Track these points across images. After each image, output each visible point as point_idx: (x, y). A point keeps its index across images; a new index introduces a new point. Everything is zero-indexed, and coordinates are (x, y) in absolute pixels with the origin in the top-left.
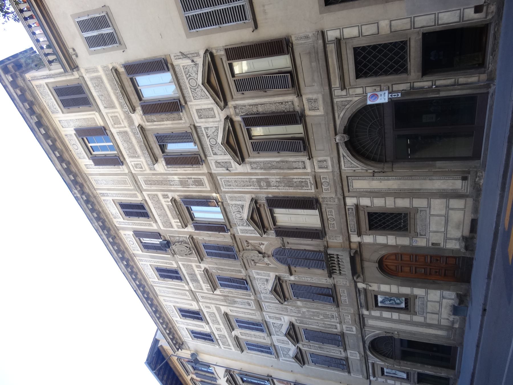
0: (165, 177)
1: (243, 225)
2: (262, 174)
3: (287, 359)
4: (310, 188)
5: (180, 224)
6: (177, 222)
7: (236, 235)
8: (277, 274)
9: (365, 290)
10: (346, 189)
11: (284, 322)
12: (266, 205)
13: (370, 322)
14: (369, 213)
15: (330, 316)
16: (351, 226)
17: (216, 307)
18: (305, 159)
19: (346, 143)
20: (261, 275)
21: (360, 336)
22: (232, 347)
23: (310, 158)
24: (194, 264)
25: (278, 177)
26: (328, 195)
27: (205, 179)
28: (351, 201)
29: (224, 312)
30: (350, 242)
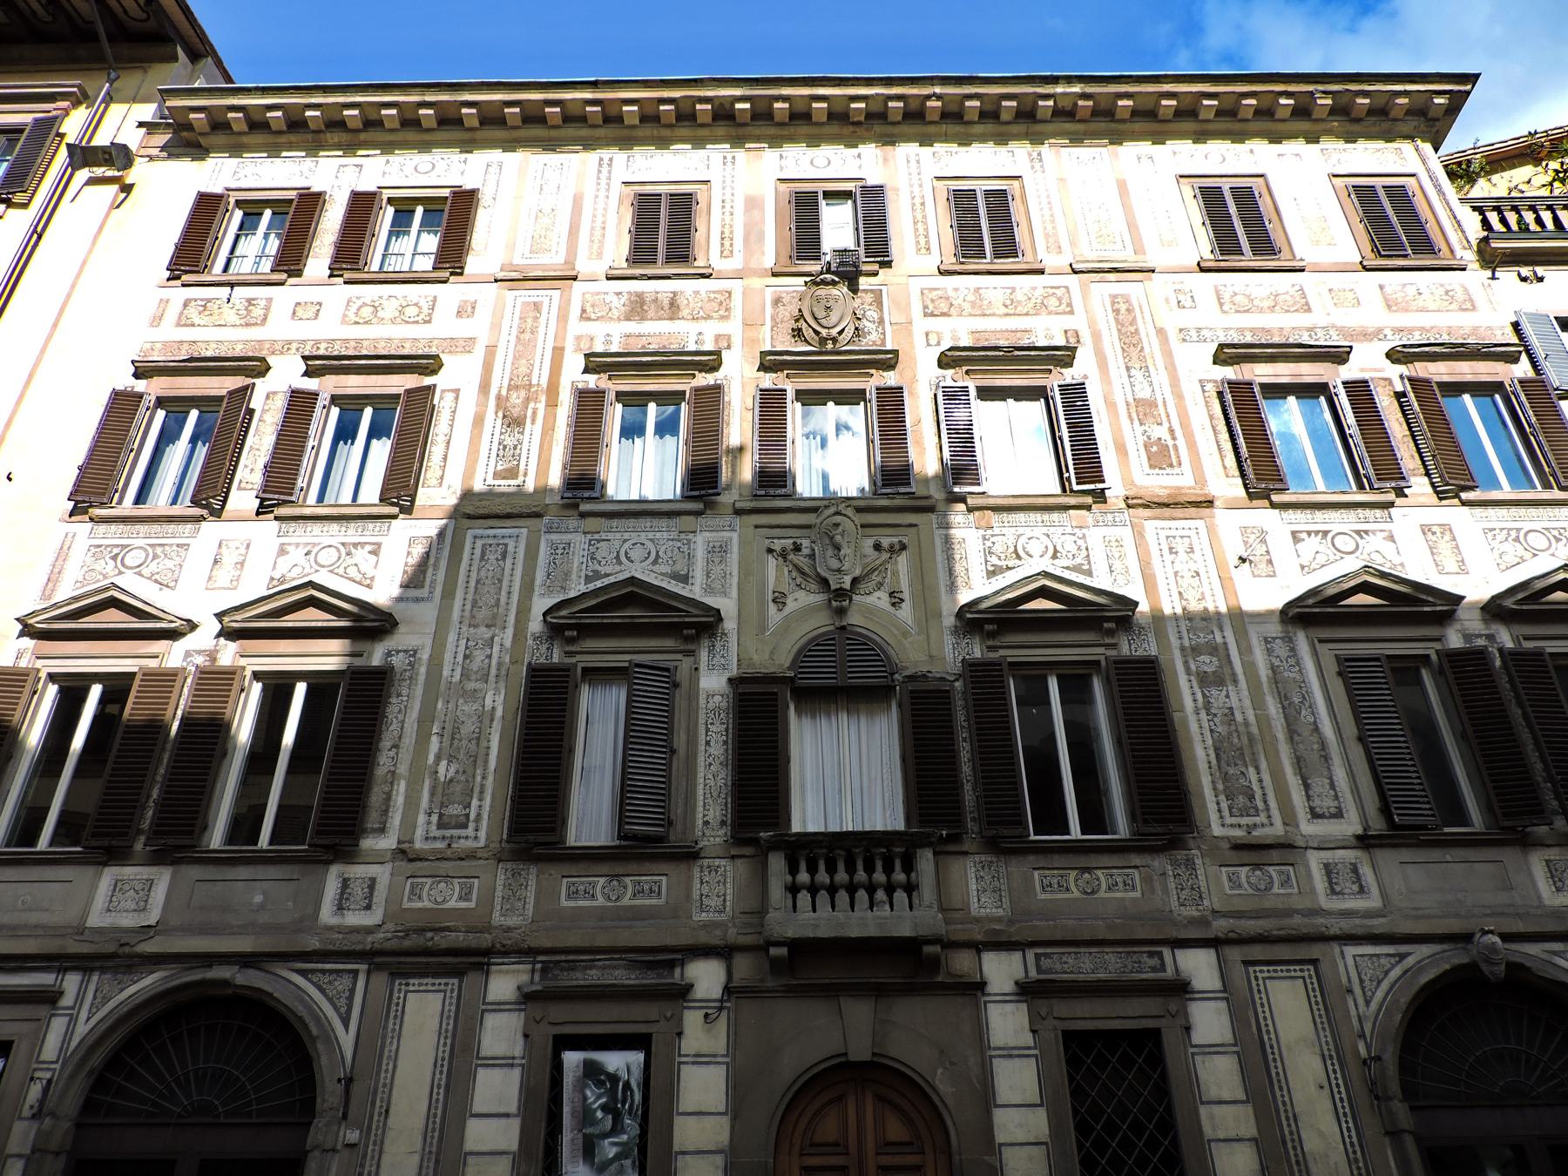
2: (1250, 668)
4: (1229, 820)
8: (730, 625)
9: (683, 992)
10: (1257, 952)
13: (424, 1010)
14: (1155, 1034)
15: (455, 810)
18: (1351, 826)
19: (1473, 967)
21: (314, 943)
23: (1364, 841)
24: (734, 327)
25: (1252, 719)
28: (1199, 966)
30: (979, 947)
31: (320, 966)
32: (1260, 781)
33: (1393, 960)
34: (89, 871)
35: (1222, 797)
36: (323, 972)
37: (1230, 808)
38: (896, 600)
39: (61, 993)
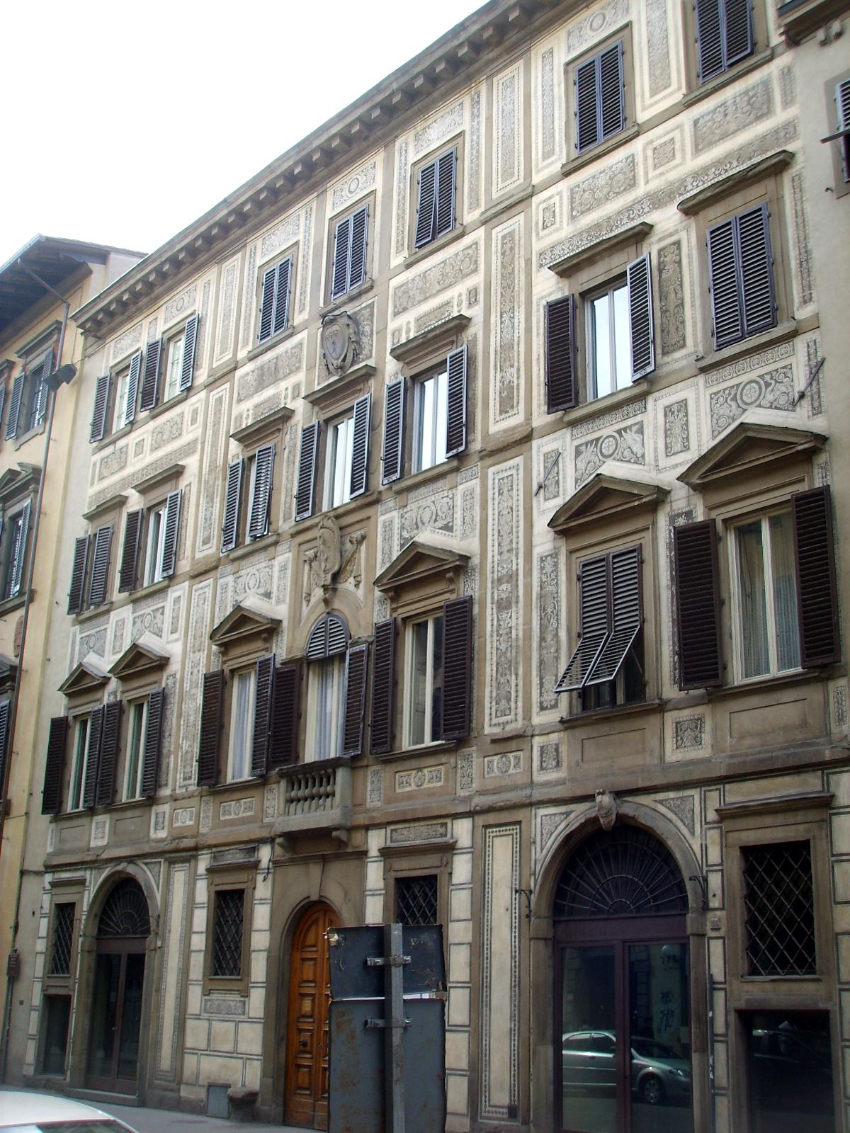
0: (523, 298)
1: (403, 528)
2: (528, 587)
3: (77, 648)
4: (495, 721)
5: (403, 340)
6: (408, 331)
7: (380, 508)
8: (285, 624)
9: (255, 866)
10: (492, 818)
11: (168, 642)
12: (453, 597)
13: (180, 877)
14: (434, 877)
16: (405, 832)
17: (196, 440)
18: (562, 711)
19: (596, 819)
20: (280, 578)
22: (97, 487)
23: (567, 724)
25: (521, 634)
26: (480, 772)
27: (515, 420)
28: (462, 831)
29: (183, 467)
30: (367, 828)
31: (153, 860)
32: (517, 685)
33: (563, 817)
34: (89, 819)
35: (494, 703)
36: (151, 863)
37: (496, 711)
38: (357, 586)
39: (85, 880)
